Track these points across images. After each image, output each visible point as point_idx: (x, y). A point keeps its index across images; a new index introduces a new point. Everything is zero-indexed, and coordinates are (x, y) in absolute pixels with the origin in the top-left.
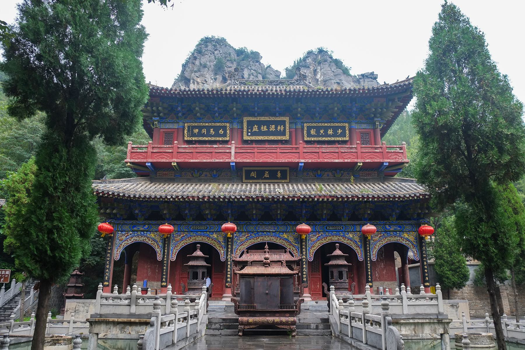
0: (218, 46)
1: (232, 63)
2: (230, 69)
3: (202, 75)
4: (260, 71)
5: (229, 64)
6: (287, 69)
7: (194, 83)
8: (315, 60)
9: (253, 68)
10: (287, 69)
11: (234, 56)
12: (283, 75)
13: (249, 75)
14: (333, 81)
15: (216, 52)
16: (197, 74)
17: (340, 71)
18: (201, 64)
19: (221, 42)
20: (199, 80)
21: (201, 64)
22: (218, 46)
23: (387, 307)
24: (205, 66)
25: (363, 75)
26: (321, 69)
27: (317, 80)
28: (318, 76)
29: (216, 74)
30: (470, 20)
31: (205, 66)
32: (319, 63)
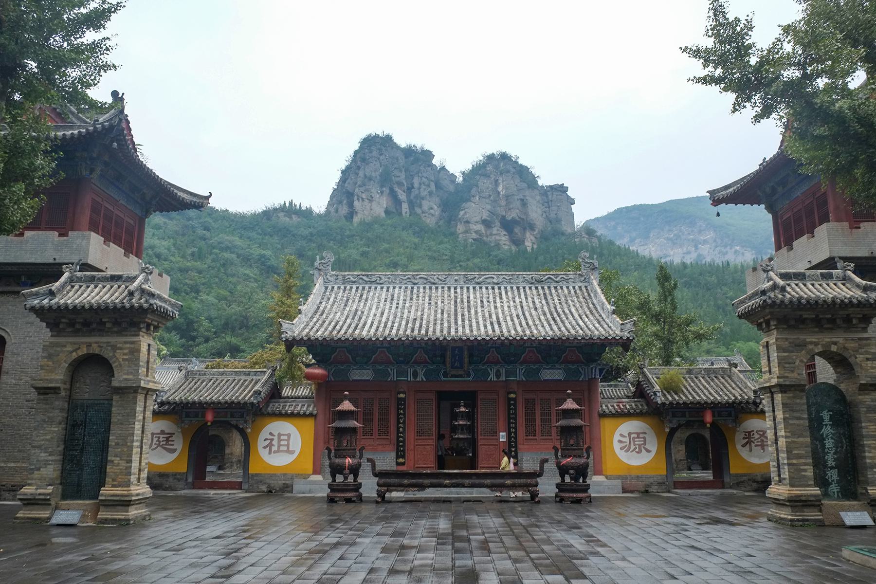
0: (384, 149)
1: (401, 171)
2: (397, 179)
3: (367, 190)
4: (433, 178)
5: (396, 172)
6: (463, 173)
7: (358, 199)
8: (496, 167)
9: (425, 175)
10: (463, 173)
11: (402, 161)
12: (460, 179)
13: (420, 184)
14: (516, 197)
15: (381, 158)
16: (362, 189)
17: (525, 185)
18: (365, 176)
19: (387, 140)
20: (364, 196)
21: (365, 176)
22: (384, 149)
23: (533, 481)
24: (370, 179)
25: (551, 187)
26: (503, 181)
27: (499, 193)
28: (500, 188)
29: (382, 186)
30: (697, 77)
31: (370, 179)
32: (501, 174)
